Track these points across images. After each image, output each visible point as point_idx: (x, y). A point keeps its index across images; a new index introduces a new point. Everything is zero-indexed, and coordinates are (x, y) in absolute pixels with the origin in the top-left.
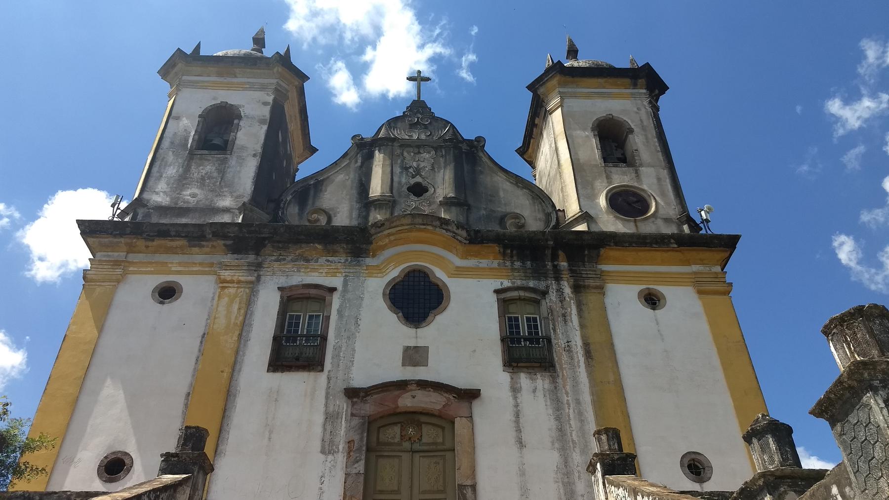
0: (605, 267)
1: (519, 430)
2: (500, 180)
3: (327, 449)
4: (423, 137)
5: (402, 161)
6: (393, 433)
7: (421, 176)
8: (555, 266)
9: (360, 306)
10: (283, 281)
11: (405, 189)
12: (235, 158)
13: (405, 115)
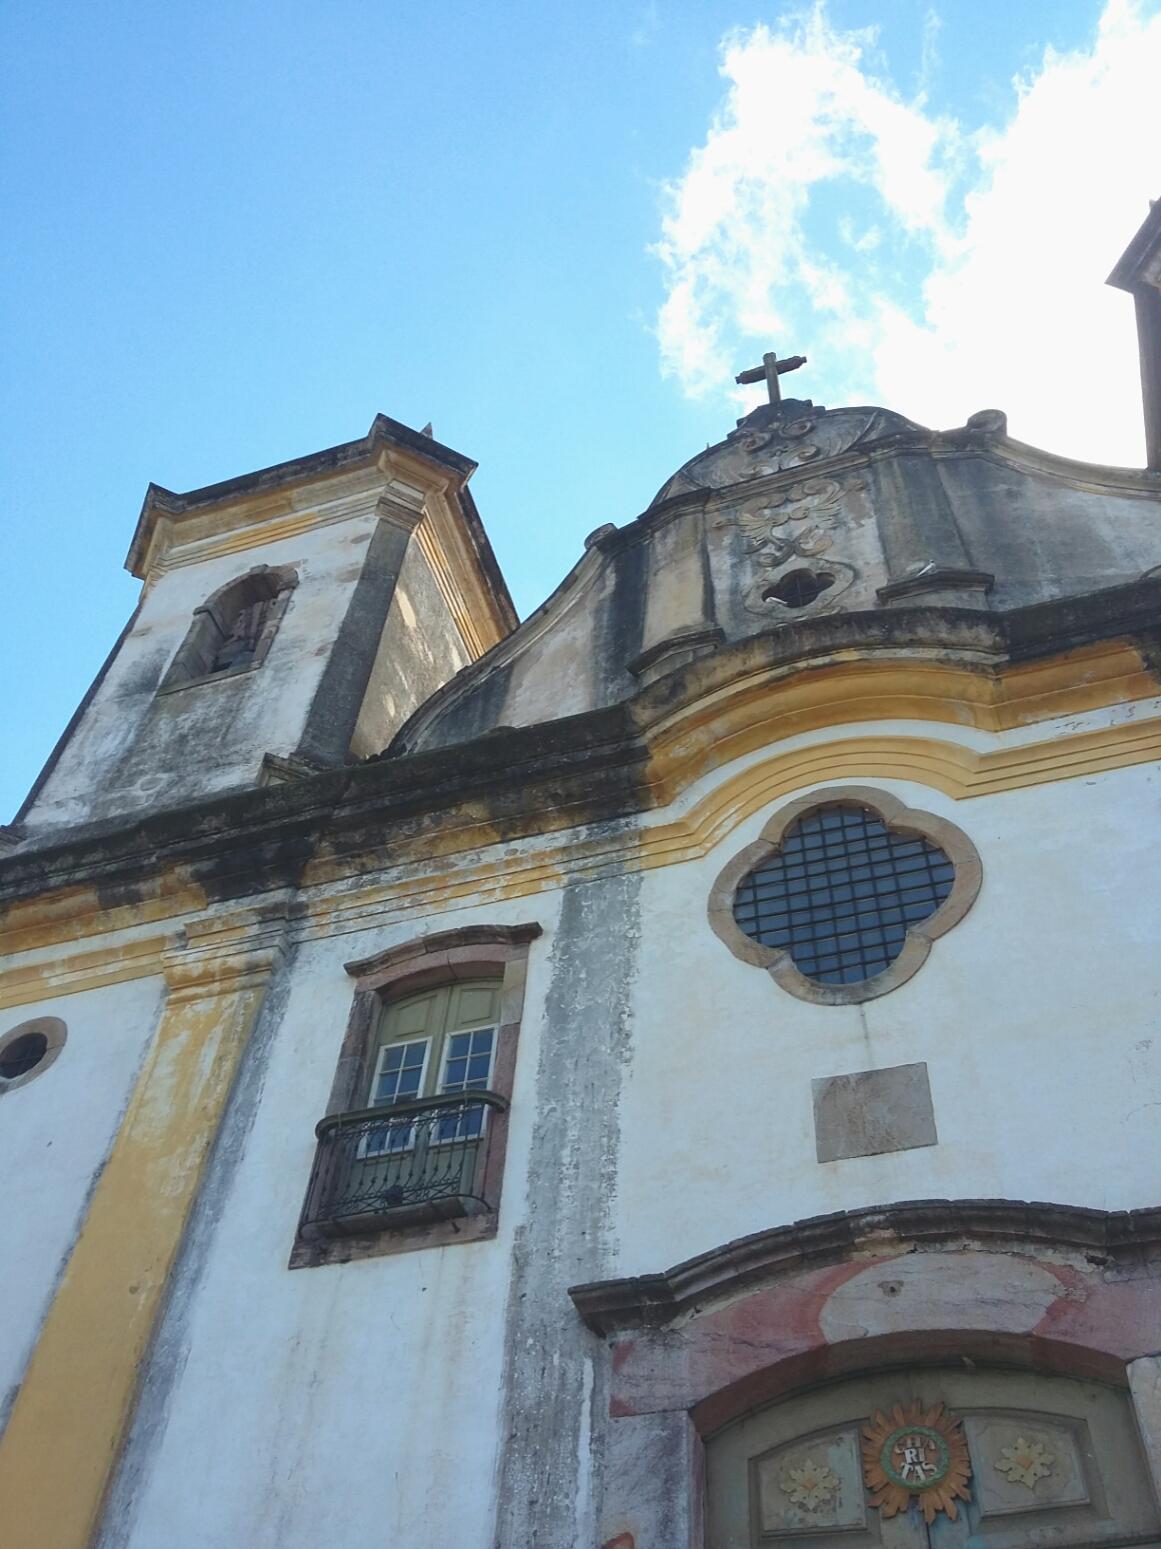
9: (628, 967)
10: (367, 945)
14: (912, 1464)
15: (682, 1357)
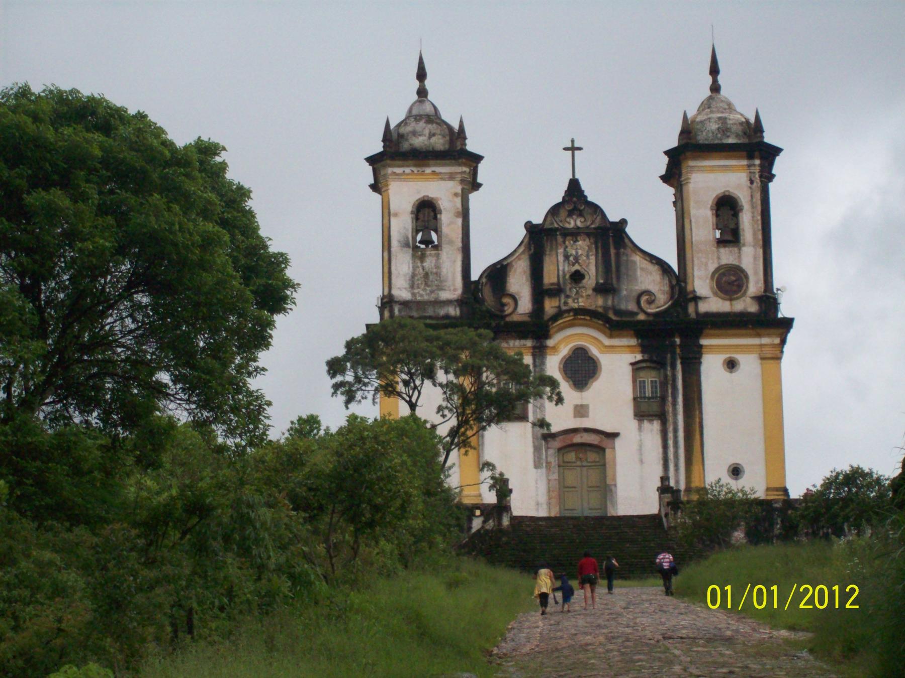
0: (704, 342)
1: (641, 454)
2: (637, 258)
3: (537, 466)
4: (579, 224)
5: (565, 250)
6: (571, 456)
7: (579, 264)
11: (567, 277)
14: (581, 455)
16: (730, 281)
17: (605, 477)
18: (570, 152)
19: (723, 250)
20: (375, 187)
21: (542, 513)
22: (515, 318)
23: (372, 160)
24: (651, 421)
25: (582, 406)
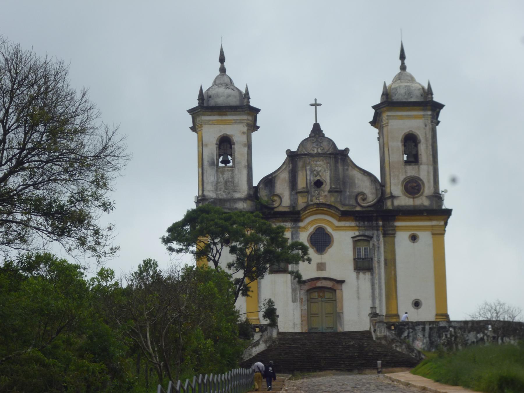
0: (397, 224)
1: (358, 294)
2: (355, 173)
3: (294, 301)
4: (319, 151)
6: (315, 295)
7: (320, 176)
8: (377, 224)
11: (312, 184)
12: (237, 170)
13: (310, 136)
15: (306, 287)
16: (413, 187)
17: (336, 307)
18: (314, 107)
19: (408, 167)
20: (194, 129)
21: (298, 330)
22: (281, 209)
23: (192, 112)
24: (364, 273)
25: (322, 263)
